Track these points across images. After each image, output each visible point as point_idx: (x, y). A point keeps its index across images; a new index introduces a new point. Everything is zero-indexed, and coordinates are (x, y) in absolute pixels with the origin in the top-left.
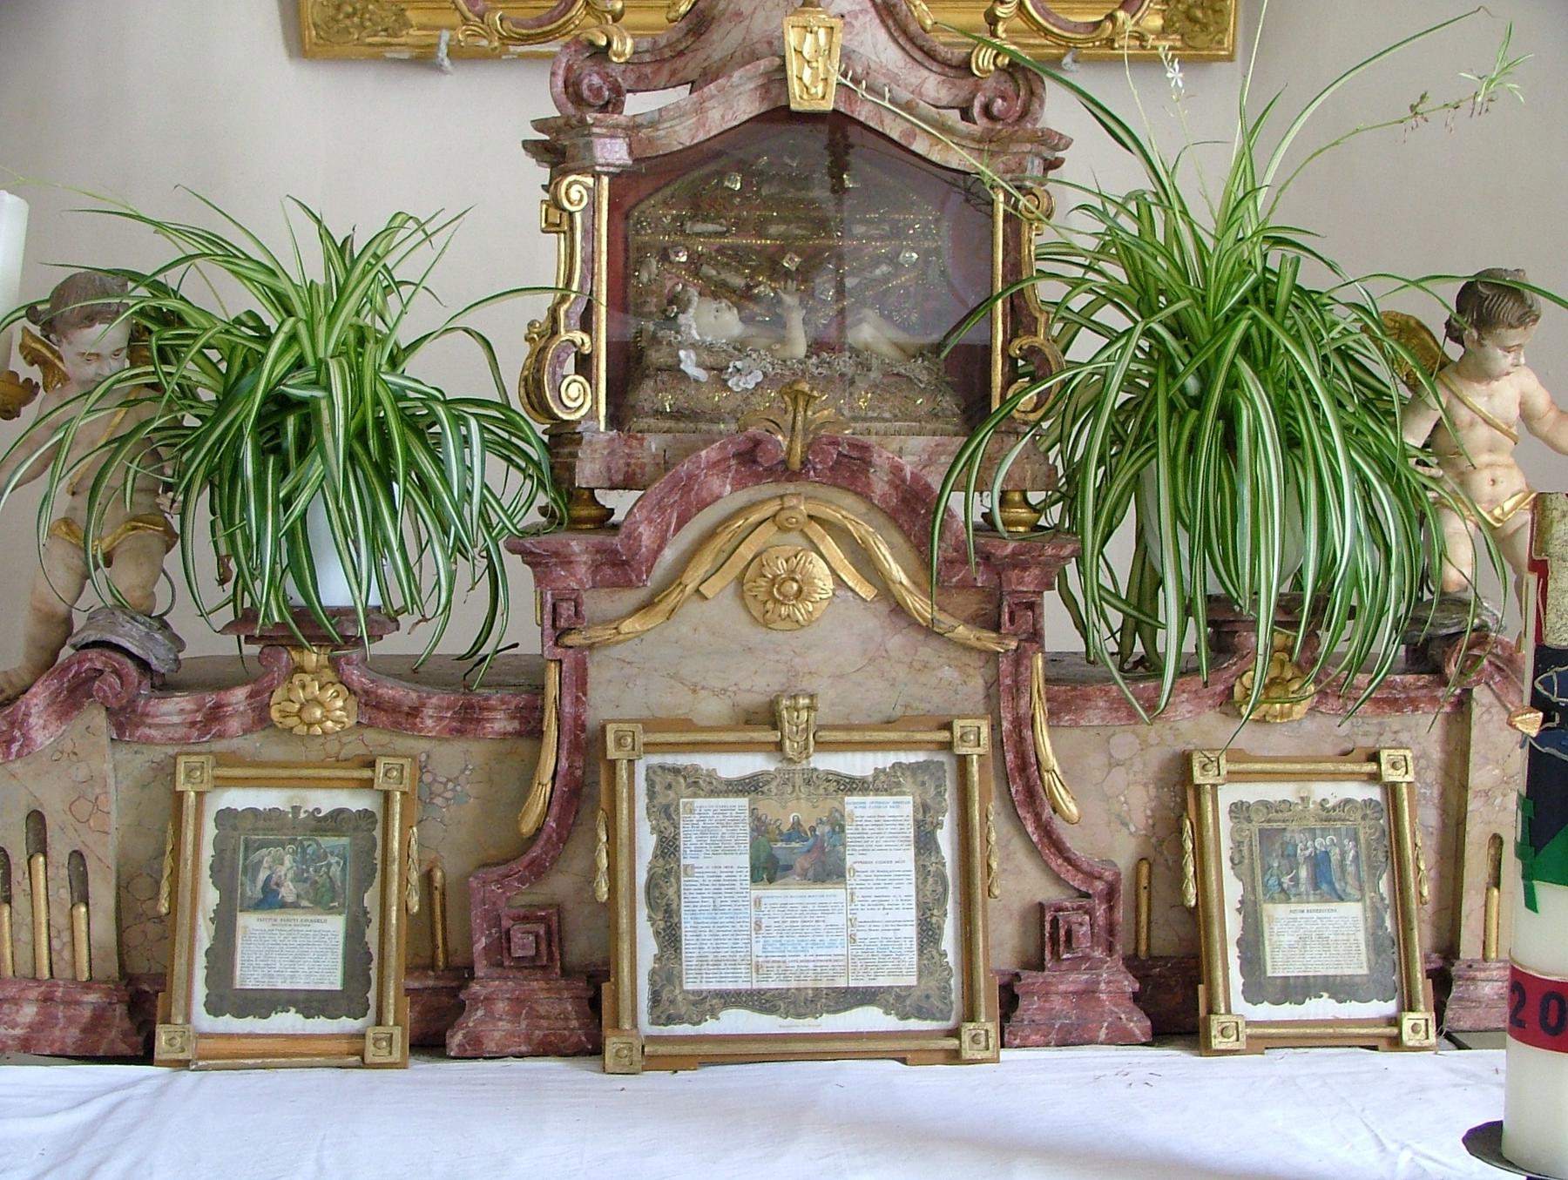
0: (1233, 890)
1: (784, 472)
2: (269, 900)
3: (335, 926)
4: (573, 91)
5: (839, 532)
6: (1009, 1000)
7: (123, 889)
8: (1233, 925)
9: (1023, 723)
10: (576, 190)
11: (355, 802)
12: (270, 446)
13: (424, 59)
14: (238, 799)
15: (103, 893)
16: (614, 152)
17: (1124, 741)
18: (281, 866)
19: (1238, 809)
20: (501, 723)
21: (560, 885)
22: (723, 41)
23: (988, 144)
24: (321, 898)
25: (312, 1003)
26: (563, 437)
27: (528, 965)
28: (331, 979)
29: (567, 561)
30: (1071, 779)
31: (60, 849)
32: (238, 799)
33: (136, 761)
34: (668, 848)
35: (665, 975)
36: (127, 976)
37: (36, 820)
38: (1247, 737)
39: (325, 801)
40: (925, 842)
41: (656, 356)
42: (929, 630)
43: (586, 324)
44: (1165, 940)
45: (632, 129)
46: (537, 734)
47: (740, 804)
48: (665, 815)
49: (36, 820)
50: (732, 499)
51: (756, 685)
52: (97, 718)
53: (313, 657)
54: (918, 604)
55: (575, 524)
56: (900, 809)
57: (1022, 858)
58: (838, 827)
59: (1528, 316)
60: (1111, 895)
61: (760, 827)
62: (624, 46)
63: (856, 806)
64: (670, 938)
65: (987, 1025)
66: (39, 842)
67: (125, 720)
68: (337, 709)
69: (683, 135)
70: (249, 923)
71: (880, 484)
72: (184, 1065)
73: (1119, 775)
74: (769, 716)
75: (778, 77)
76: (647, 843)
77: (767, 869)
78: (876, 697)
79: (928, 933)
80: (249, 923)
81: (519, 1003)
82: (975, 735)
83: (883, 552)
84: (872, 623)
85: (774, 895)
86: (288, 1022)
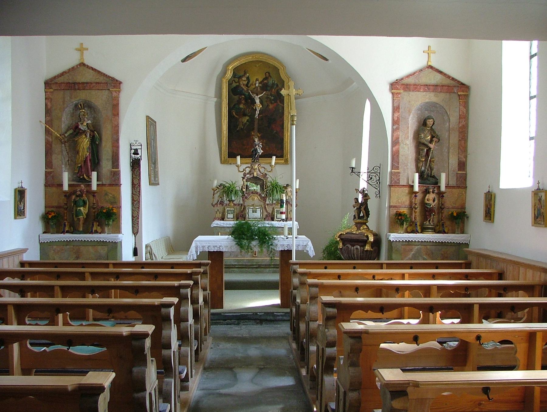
0: (276, 214)
1: (254, 193)
2: (229, 214)
3: (233, 215)
4: (244, 175)
5: (256, 196)
6: (265, 219)
7: (222, 213)
8: (276, 215)
9: (265, 205)
10: (244, 180)
11: (233, 209)
12: (230, 192)
13: (231, 164)
14: (228, 209)
15: (221, 213)
16: (246, 178)
17: (271, 207)
18: (230, 212)
19: (276, 210)
20: (240, 205)
21: (243, 213)
22: (251, 173)
23: (264, 178)
24: (232, 214)
25: (231, 218)
26: (243, 192)
27: (241, 217)
28: (232, 217)
29: (244, 197)
30: (268, 208)
31: (219, 211)
32: (228, 209)
33: (223, 207)
34: (248, 211)
35: (248, 217)
36: (222, 218)
37: (218, 210)
38: (277, 206)
39: (232, 209)
40: (261, 211)
41: (248, 188)
42: (261, 201)
43: (245, 186)
44: (273, 217)
45: (247, 177)
46: (242, 206)
47: (252, 209)
48: (248, 210)
49: (218, 210)
50: (251, 195)
51: (253, 203)
52: (221, 205)
53: (232, 202)
54: (261, 200)
55: (244, 196)
56: (260, 209)
57: (266, 212)
58: (256, 210)
59: (289, 186)
60: (270, 214)
61: (253, 210)
62: (246, 173)
63: (257, 209)
64: (248, 215)
65: (263, 220)
66: (218, 211)
67: (222, 205)
68: (233, 205)
69: (249, 177)
70: (228, 215)
71: (258, 194)
72: (225, 221)
73: (270, 208)
74: (253, 205)
75: (254, 175)
76: (247, 211)
77: (253, 212)
78: (258, 204)
79: (261, 215)
80: (228, 215)
81: (241, 219)
82: (263, 206)
83: (259, 197)
84: (258, 201)
85: (253, 213)
86: (230, 219)
